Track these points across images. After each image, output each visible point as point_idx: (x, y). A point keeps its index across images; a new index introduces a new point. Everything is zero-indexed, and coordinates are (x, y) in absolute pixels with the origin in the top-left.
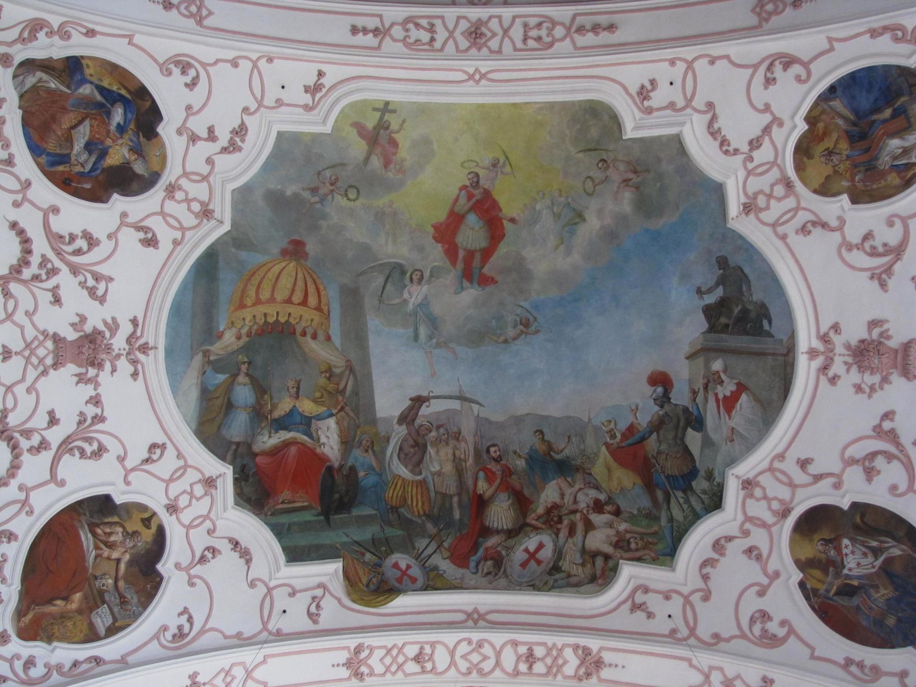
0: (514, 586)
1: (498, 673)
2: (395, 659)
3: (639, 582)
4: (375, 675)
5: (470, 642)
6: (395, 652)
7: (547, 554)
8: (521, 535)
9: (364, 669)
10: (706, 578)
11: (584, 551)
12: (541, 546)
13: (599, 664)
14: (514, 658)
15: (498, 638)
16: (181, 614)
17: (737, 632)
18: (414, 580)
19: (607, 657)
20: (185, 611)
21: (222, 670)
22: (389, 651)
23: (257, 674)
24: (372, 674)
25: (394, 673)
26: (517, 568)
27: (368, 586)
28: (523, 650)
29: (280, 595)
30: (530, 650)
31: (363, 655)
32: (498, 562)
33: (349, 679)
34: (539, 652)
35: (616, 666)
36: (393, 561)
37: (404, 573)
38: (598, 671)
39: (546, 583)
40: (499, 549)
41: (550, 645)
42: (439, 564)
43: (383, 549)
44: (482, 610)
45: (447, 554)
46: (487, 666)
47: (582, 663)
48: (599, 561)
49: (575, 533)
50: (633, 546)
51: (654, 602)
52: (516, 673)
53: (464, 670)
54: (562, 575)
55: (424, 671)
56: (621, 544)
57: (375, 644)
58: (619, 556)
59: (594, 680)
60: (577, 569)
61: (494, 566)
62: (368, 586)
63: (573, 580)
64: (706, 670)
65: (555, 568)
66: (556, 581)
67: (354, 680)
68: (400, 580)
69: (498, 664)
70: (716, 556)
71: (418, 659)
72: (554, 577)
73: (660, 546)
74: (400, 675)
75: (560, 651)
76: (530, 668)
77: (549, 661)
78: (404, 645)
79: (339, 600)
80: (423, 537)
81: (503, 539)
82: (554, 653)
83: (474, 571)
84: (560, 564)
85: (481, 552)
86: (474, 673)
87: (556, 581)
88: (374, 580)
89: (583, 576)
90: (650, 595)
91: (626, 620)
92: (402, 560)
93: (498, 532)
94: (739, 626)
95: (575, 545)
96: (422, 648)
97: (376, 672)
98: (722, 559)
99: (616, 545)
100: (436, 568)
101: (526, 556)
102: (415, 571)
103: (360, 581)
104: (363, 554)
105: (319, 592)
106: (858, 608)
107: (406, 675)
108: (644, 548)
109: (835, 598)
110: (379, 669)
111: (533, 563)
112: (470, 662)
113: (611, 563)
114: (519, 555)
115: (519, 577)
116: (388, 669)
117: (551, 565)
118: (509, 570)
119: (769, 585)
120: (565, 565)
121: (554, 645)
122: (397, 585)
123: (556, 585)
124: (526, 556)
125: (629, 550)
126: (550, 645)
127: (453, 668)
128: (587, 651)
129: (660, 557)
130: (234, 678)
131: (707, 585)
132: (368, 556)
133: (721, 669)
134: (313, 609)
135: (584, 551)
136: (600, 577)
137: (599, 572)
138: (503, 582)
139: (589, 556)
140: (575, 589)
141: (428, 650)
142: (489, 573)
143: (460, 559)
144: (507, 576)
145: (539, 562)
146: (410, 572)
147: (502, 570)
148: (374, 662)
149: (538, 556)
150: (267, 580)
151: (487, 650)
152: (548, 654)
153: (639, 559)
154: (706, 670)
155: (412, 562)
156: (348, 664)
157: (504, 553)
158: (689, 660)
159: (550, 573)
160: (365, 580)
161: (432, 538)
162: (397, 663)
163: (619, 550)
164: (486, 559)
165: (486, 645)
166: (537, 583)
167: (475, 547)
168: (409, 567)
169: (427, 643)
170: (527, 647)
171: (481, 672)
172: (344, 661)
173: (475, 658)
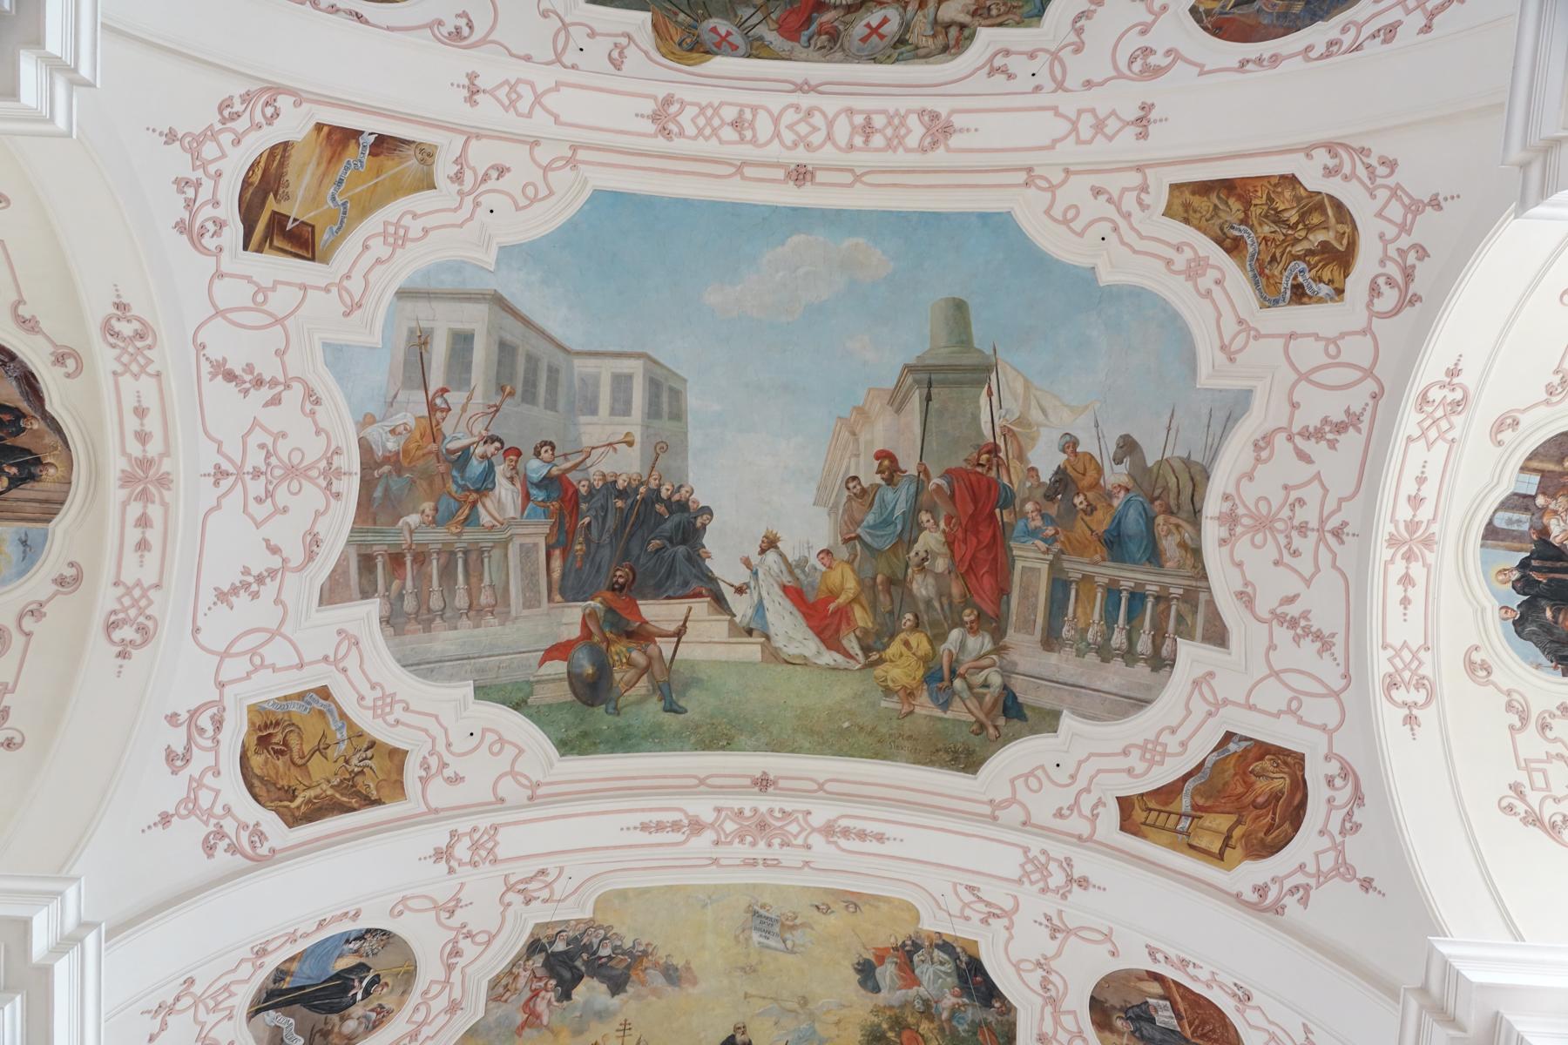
0: (850, 57)
1: (829, 146)
2: (709, 121)
3: (999, 47)
4: (685, 137)
5: (797, 108)
6: (709, 112)
7: (892, 28)
8: (863, 10)
9: (672, 127)
10: (1079, 32)
11: (935, 22)
12: (885, 21)
13: (948, 130)
14: (848, 129)
15: (831, 105)
16: (458, 16)
17: (1114, 74)
18: (735, 48)
19: (958, 121)
20: (464, 15)
21: (506, 82)
22: (702, 110)
23: (547, 100)
24: (681, 134)
25: (707, 139)
26: (857, 43)
27: (680, 44)
28: (859, 120)
29: (579, 36)
30: (868, 120)
31: (674, 109)
32: (834, 36)
33: (655, 136)
34: (879, 121)
35: (968, 130)
36: (712, 25)
37: (724, 39)
38: (946, 139)
39: (889, 57)
40: (836, 24)
41: (892, 111)
42: (764, 35)
43: (700, 12)
44: (813, 83)
45: (776, 26)
46: (816, 139)
47: (928, 130)
48: (953, 32)
49: (926, 5)
50: (994, 12)
51: (1013, 63)
52: (851, 147)
53: (789, 143)
54: (908, 48)
55: (742, 139)
56: (979, 12)
57: (688, 99)
58: (977, 23)
59: (941, 150)
60: (927, 41)
61: (829, 41)
62: (680, 44)
63: (921, 52)
64: (1074, 117)
65: (902, 41)
66: (902, 53)
67: (660, 137)
68: (718, 45)
69: (829, 137)
70: (1093, 7)
71: (736, 124)
72: (898, 51)
73: (1026, 9)
74: (714, 141)
75: (904, 117)
76: (867, 141)
77: (889, 132)
78: (722, 104)
79: (646, 53)
80: (747, 6)
81: (842, 14)
82: (896, 121)
83: (806, 45)
84: (907, 37)
85: (814, 27)
86: (801, 147)
87: (902, 53)
88: (688, 40)
89: (933, 47)
90: (1012, 57)
91: (981, 82)
92: (723, 26)
93: (835, 7)
94: (1116, 67)
95: (925, 17)
96: (741, 113)
97: (686, 133)
98: (1100, 9)
99: (974, 14)
100: (761, 38)
101: (867, 31)
102: (736, 38)
103: (671, 39)
104: (676, 14)
105: (624, 41)
106: (1259, 11)
107: (721, 142)
108: (1007, 13)
109: (1235, 10)
110: (691, 130)
111: (875, 38)
112: (797, 133)
113: (967, 32)
114: (859, 30)
115: (858, 50)
116: (700, 131)
117: (896, 39)
118: (846, 45)
119: (1154, 22)
120: (912, 38)
121: (897, 110)
122: (715, 49)
123: (901, 57)
124: (867, 31)
125: (990, 16)
126: (892, 111)
127: (776, 141)
128: (935, 116)
129: (1026, 20)
130: (520, 97)
131: (1080, 38)
132: (682, 16)
133: (1093, 111)
134: (615, 54)
135: (935, 22)
136: (954, 46)
137: (952, 43)
138: (839, 55)
139: (941, 27)
140: (924, 60)
141: (748, 115)
142: (823, 47)
143: (790, 33)
144: (844, 50)
145: (882, 37)
146: (730, 39)
147: (838, 45)
148: (685, 119)
149: (882, 31)
150: (561, 13)
151: (818, 120)
152: (890, 123)
153: (1000, 25)
154: (1074, 117)
155: (733, 29)
156: (655, 117)
157: (841, 27)
158: (1055, 110)
159: (894, 47)
160: (677, 39)
161: (758, 8)
162: (712, 126)
163: (978, 18)
164: (820, 34)
165: (817, 114)
166: (878, 56)
167: (808, 21)
168: (729, 34)
169: (748, 106)
170: (864, 116)
171: (808, 146)
172: (650, 113)
173: (803, 129)
